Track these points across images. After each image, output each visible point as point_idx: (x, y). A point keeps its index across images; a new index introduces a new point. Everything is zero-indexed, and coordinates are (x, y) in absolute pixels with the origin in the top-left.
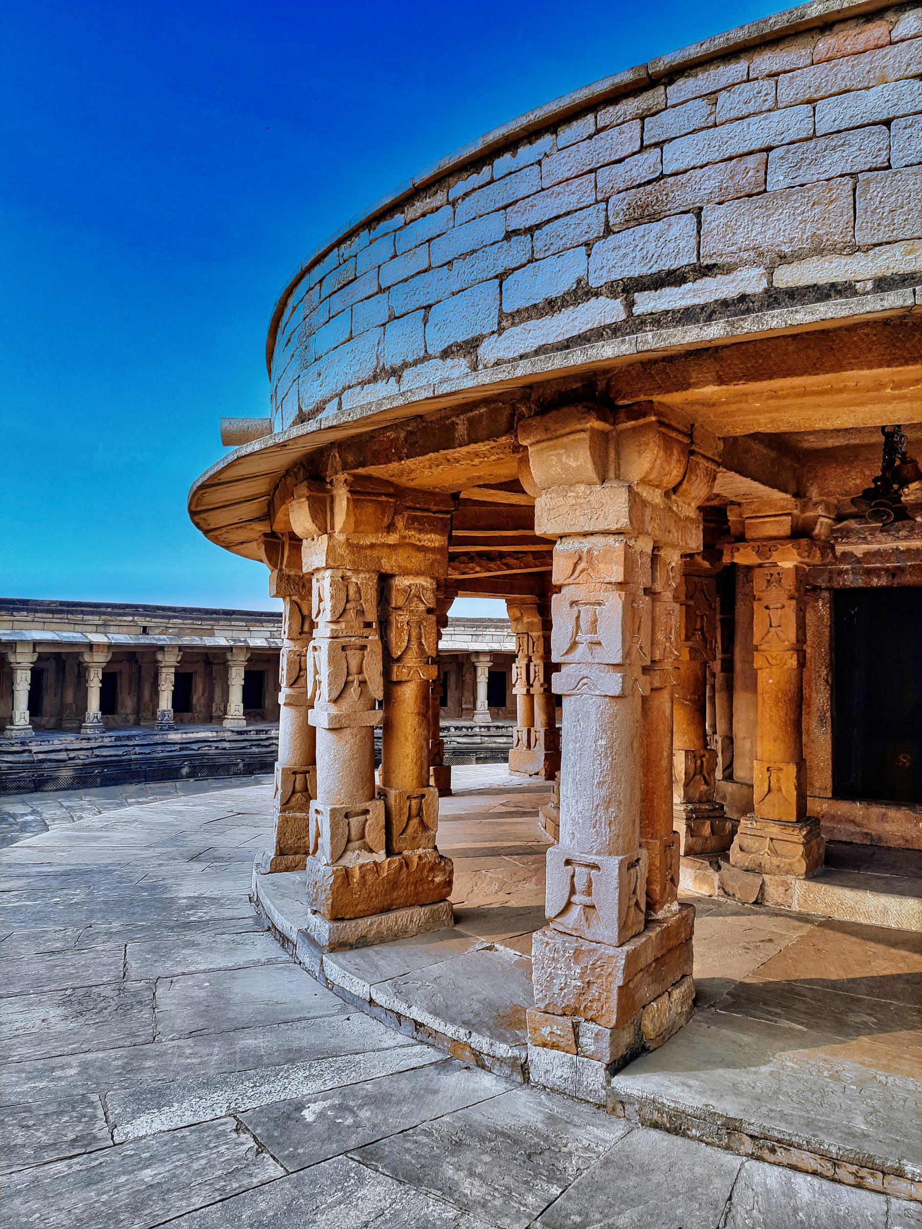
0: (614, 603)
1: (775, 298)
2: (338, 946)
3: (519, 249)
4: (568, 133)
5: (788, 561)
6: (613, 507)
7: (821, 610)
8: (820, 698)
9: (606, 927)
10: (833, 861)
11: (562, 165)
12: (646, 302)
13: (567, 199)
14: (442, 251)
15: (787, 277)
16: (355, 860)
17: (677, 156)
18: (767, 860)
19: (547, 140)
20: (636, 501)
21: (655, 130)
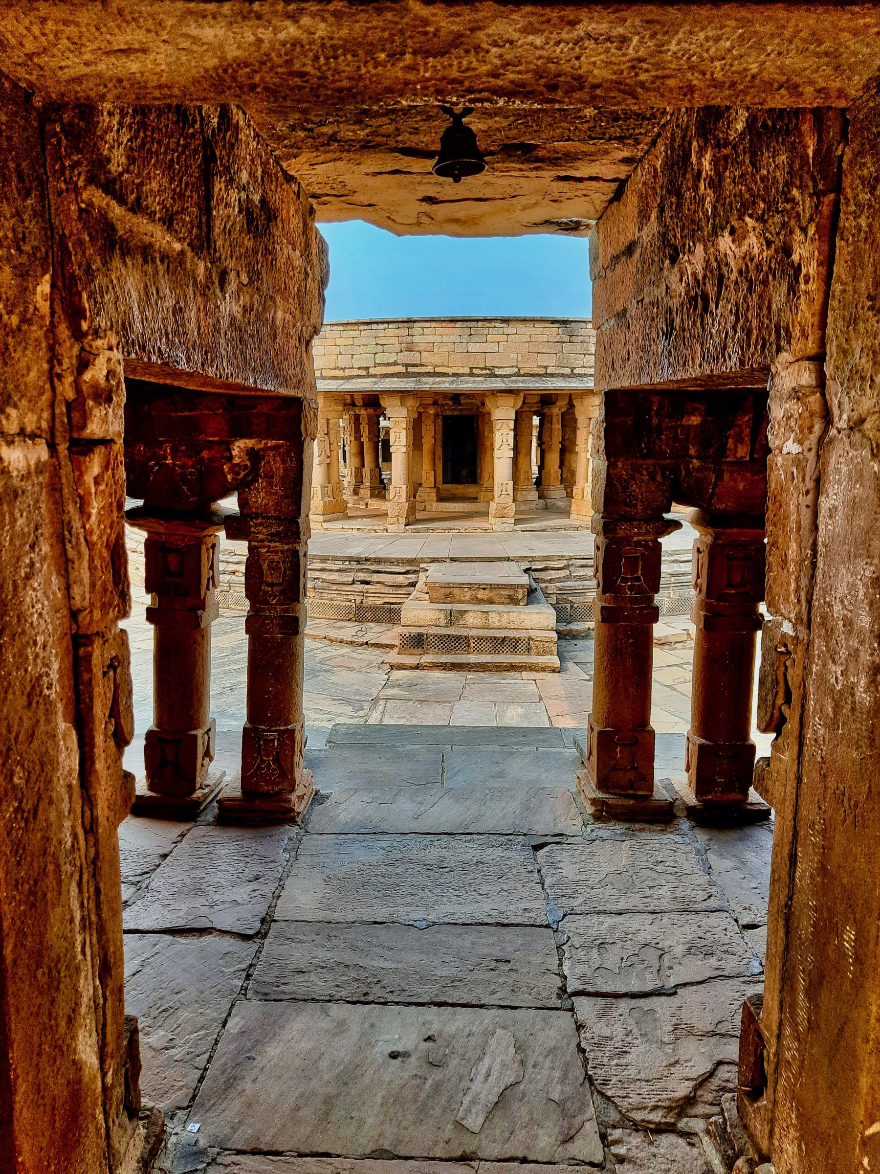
0: (404, 432)
1: (436, 374)
2: (325, 521)
4: (391, 326)
6: (404, 412)
7: (440, 422)
8: (439, 452)
9: (403, 499)
10: (441, 499)
11: (389, 332)
12: (410, 369)
13: (392, 341)
14: (357, 342)
15: (437, 370)
16: (327, 499)
17: (416, 339)
18: (426, 498)
19: (386, 326)
21: (412, 331)
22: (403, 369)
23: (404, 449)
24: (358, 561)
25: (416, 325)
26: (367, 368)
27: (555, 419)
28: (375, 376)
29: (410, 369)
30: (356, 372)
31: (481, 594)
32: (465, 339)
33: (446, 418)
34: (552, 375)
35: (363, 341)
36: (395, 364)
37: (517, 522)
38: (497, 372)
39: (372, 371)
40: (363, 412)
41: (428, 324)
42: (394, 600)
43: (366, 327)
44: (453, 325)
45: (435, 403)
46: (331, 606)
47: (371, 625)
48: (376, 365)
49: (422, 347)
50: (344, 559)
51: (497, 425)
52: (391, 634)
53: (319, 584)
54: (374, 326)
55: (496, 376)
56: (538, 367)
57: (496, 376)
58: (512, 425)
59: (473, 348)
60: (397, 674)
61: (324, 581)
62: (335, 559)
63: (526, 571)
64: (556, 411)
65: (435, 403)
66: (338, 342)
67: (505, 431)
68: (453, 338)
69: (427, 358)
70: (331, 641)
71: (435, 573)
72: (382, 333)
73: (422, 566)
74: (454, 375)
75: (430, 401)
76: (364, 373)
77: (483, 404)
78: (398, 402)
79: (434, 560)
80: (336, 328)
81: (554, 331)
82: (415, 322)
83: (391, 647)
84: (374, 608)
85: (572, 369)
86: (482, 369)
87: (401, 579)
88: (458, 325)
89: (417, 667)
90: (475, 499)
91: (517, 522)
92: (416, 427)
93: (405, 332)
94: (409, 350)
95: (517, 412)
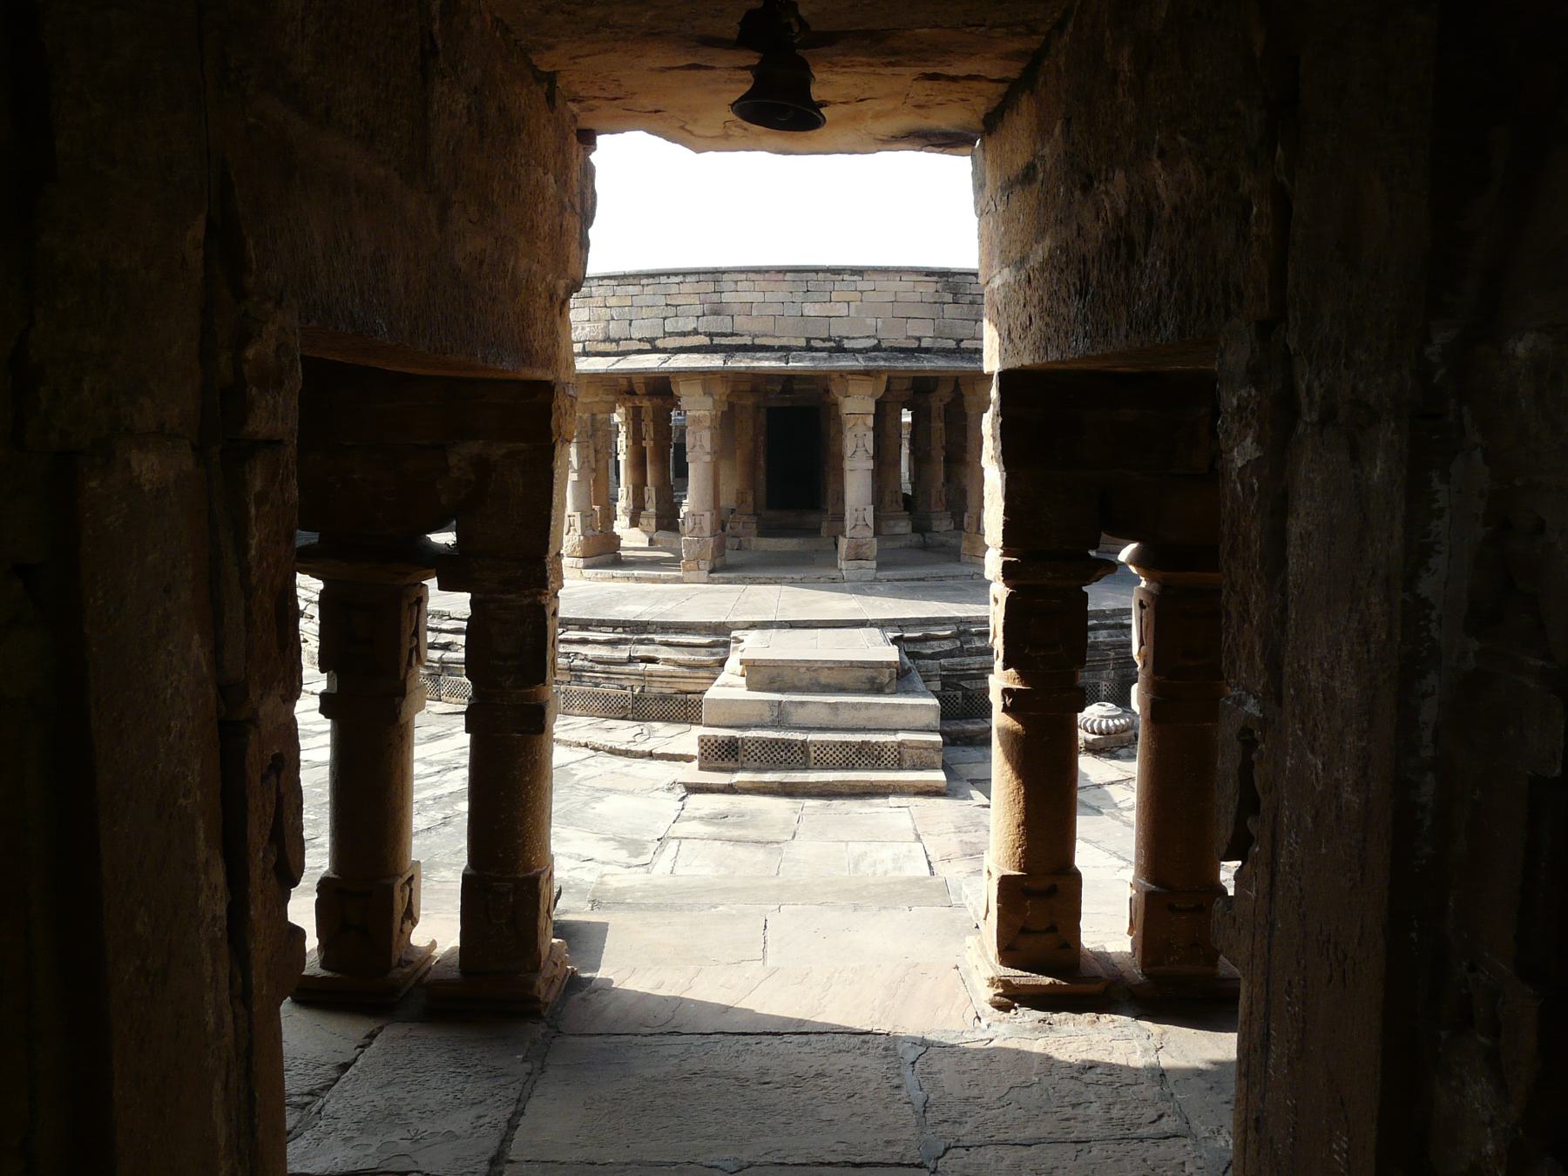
3: (671, 311)
4: (688, 279)
5: (749, 401)
6: (709, 402)
10: (766, 531)
11: (686, 288)
14: (638, 301)
15: (758, 341)
17: (726, 297)
19: (679, 279)
20: (714, 401)
22: (705, 340)
23: (708, 458)
25: (725, 277)
26: (655, 339)
27: (934, 414)
28: (664, 351)
29: (717, 341)
30: (636, 345)
31: (824, 677)
32: (799, 297)
33: (772, 413)
34: (927, 350)
35: (649, 300)
36: (695, 332)
37: (880, 567)
38: (847, 344)
39: (660, 344)
40: (646, 404)
41: (743, 276)
42: (691, 688)
43: (651, 281)
44: (780, 276)
45: (754, 390)
46: (596, 696)
47: (657, 725)
48: (667, 335)
49: (736, 309)
50: (615, 625)
51: (849, 423)
52: (687, 739)
53: (577, 663)
54: (664, 279)
55: (845, 350)
56: (908, 338)
57: (845, 350)
58: (870, 421)
59: (810, 310)
60: (695, 799)
61: (586, 659)
62: (601, 624)
63: (895, 641)
64: (937, 402)
65: (754, 390)
66: (612, 302)
67: (860, 430)
68: (780, 296)
69: (741, 324)
70: (596, 749)
71: (753, 646)
72: (674, 289)
73: (734, 634)
74: (782, 348)
75: (747, 387)
76: (648, 346)
77: (827, 391)
78: (699, 390)
79: (753, 626)
80: (606, 282)
81: (929, 288)
82: (724, 272)
83: (687, 759)
84: (664, 698)
86: (824, 340)
87: (703, 657)
88: (789, 276)
89: (730, 789)
90: (814, 532)
91: (880, 567)
92: (727, 422)
93: (711, 287)
94: (716, 313)
95: (877, 403)
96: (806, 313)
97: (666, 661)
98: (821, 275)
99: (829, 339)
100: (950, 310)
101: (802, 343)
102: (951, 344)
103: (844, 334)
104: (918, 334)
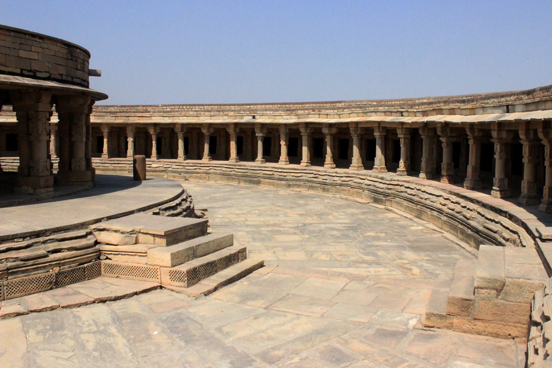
24: (38, 234)
31: (190, 233)
38: (38, 75)
46: (31, 281)
50: (23, 236)
53: (9, 264)
56: (59, 74)
59: (22, 54)
61: (17, 259)
81: (64, 51)
85: (73, 78)
86: (29, 71)
88: (12, 34)
96: (21, 55)
97: (70, 249)
98: (27, 37)
99: (30, 71)
100: (71, 63)
101: (18, 71)
102: (70, 79)
103: (37, 69)
104: (62, 73)
